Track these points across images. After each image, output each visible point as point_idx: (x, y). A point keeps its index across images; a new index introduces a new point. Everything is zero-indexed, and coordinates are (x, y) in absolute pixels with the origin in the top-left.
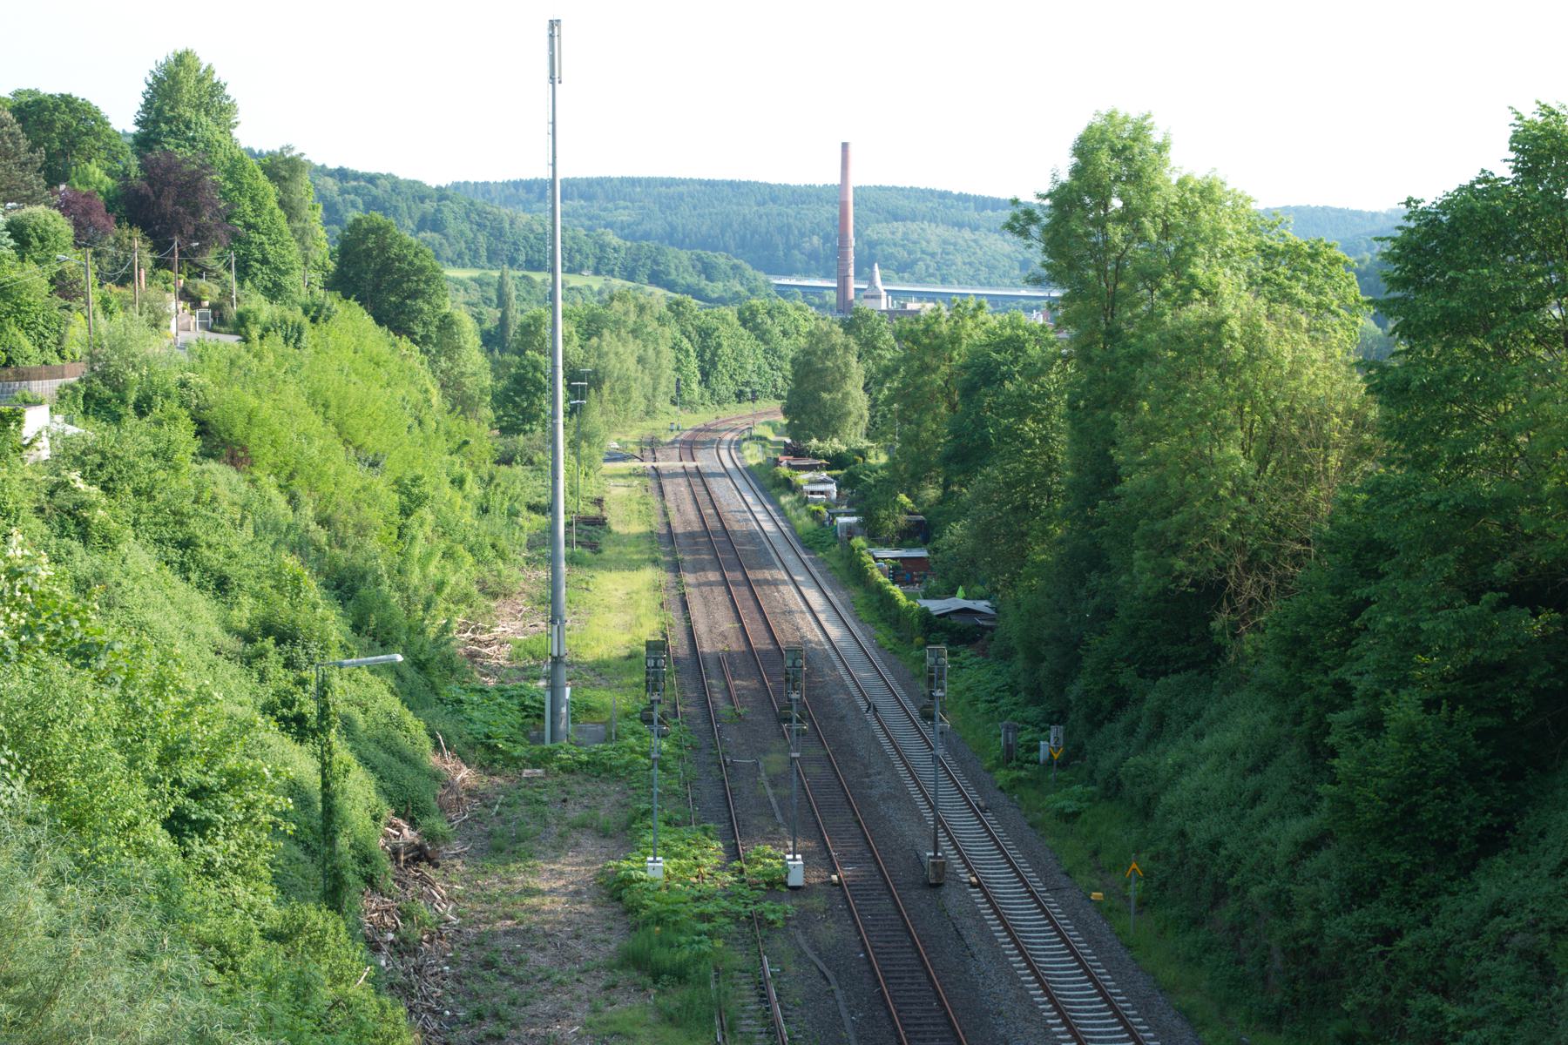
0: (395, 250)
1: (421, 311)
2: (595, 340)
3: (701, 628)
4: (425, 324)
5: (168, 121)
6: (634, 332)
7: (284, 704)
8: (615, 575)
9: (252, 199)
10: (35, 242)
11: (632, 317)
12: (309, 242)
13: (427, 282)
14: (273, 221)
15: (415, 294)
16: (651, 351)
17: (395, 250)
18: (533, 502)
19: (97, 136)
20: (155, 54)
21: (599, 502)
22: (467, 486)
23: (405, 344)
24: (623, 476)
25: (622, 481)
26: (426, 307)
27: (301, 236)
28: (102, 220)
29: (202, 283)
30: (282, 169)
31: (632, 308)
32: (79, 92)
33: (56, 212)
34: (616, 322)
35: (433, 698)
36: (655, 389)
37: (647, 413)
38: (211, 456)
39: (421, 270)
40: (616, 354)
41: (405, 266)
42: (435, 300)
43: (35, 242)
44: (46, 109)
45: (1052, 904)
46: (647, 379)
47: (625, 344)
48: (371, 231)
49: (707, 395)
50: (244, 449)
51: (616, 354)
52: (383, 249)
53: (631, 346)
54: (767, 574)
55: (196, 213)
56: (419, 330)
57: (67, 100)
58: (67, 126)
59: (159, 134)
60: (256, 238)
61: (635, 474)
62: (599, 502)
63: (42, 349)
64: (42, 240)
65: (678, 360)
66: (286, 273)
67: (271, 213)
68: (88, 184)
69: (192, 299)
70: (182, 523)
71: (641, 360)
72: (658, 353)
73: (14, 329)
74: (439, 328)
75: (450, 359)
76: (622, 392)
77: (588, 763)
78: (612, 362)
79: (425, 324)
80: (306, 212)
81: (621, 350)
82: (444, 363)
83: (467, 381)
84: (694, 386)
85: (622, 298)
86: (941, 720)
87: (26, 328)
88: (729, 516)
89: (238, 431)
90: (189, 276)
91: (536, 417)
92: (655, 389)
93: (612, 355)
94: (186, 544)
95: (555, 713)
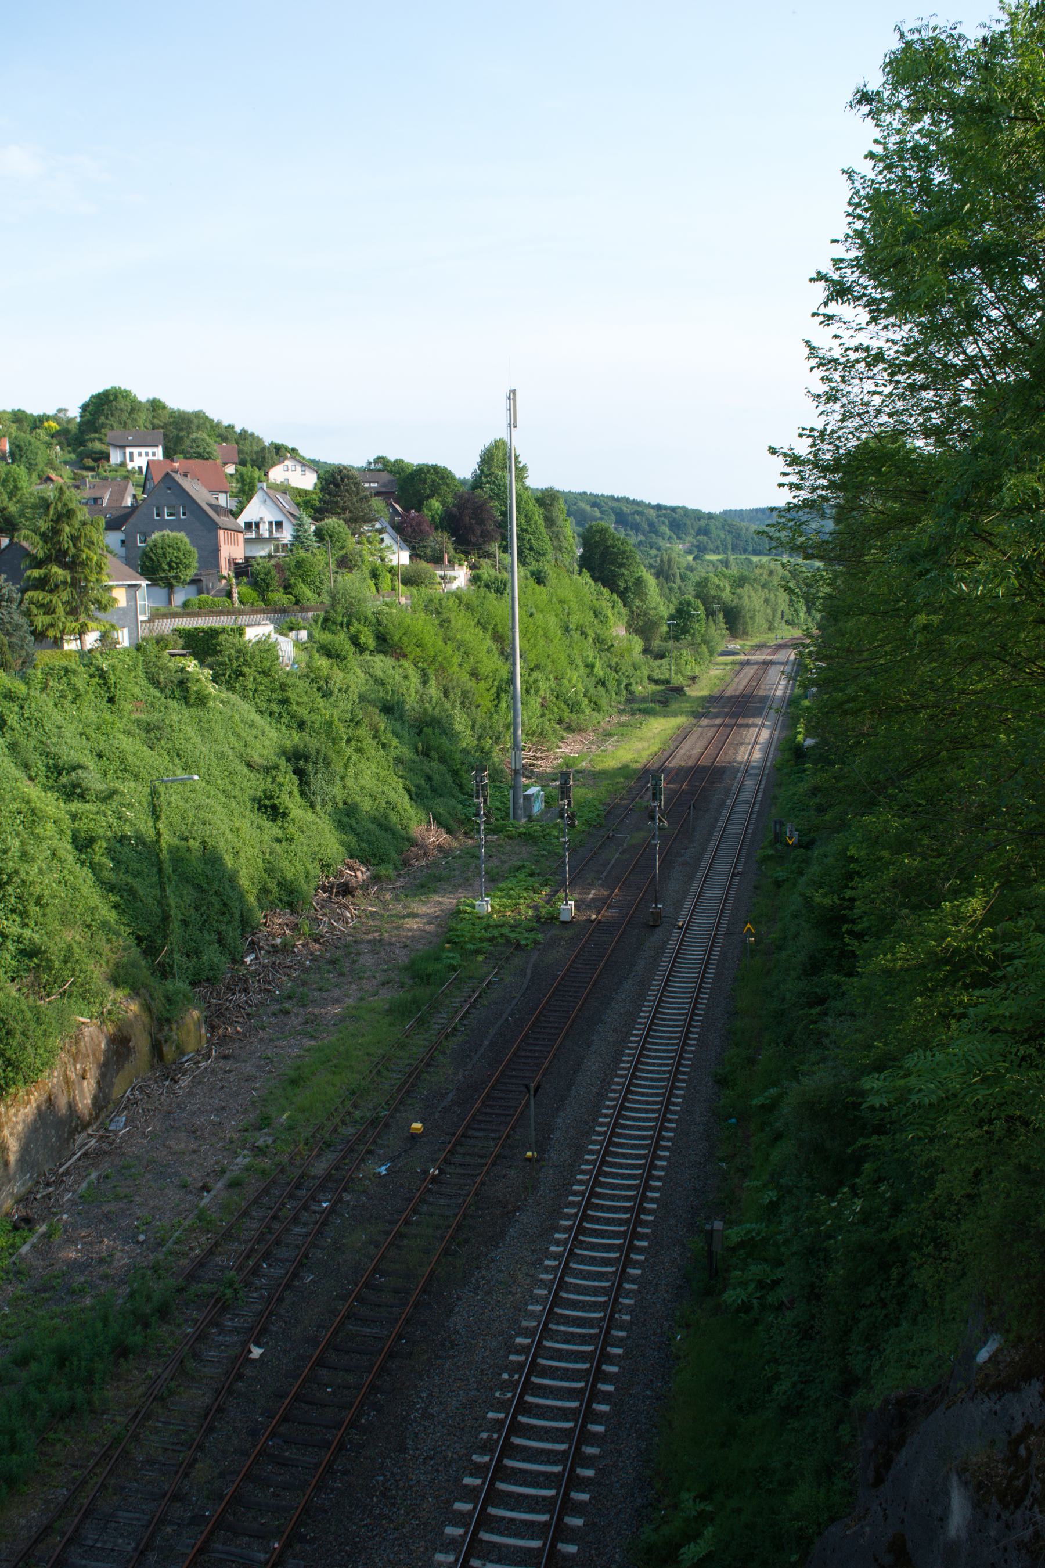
0: (610, 542)
1: (623, 574)
2: (738, 591)
3: (682, 752)
4: (626, 581)
5: (486, 476)
6: (764, 586)
7: (266, 798)
8: (662, 720)
9: (526, 516)
10: (327, 538)
11: (765, 577)
12: (562, 538)
13: (627, 558)
14: (537, 528)
15: (622, 565)
16: (772, 595)
17: (610, 542)
18: (656, 678)
19: (448, 485)
20: (487, 442)
21: (693, 679)
22: (596, 669)
23: (606, 592)
24: (726, 664)
25: (722, 667)
26: (626, 572)
27: (555, 536)
28: (427, 528)
29: (485, 562)
30: (547, 499)
31: (765, 572)
32: (441, 463)
33: (341, 522)
34: (755, 580)
35: (456, 791)
36: (774, 616)
37: (770, 629)
38: (383, 652)
39: (624, 552)
40: (749, 597)
41: (615, 550)
42: (631, 569)
43: (327, 538)
44: (423, 473)
45: (720, 941)
46: (769, 611)
47: (756, 591)
48: (597, 531)
49: (810, 620)
50: (401, 648)
51: (749, 597)
52: (605, 540)
53: (760, 593)
54: (751, 721)
55: (481, 522)
56: (622, 585)
57: (435, 469)
58: (433, 481)
59: (482, 483)
60: (527, 537)
61: (733, 663)
62: (693, 679)
63: (319, 594)
64: (331, 537)
65: (791, 601)
66: (544, 555)
67: (536, 523)
68: (431, 510)
69: (472, 567)
70: (283, 690)
71: (767, 601)
72: (776, 596)
73: (302, 585)
74: (635, 584)
75: (642, 600)
76: (751, 618)
77: (525, 833)
78: (746, 601)
79: (626, 581)
80: (560, 522)
81: (753, 594)
82: (637, 602)
83: (651, 612)
84: (802, 615)
85: (762, 566)
86: (660, 820)
87: (309, 584)
88: (763, 687)
89: (396, 639)
90: (479, 557)
91: (688, 632)
92: (774, 616)
93: (746, 597)
94: (284, 702)
95: (515, 803)
